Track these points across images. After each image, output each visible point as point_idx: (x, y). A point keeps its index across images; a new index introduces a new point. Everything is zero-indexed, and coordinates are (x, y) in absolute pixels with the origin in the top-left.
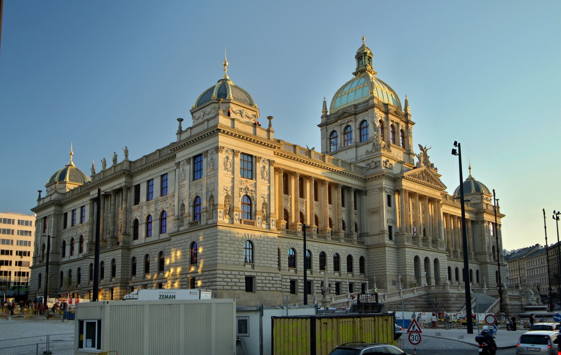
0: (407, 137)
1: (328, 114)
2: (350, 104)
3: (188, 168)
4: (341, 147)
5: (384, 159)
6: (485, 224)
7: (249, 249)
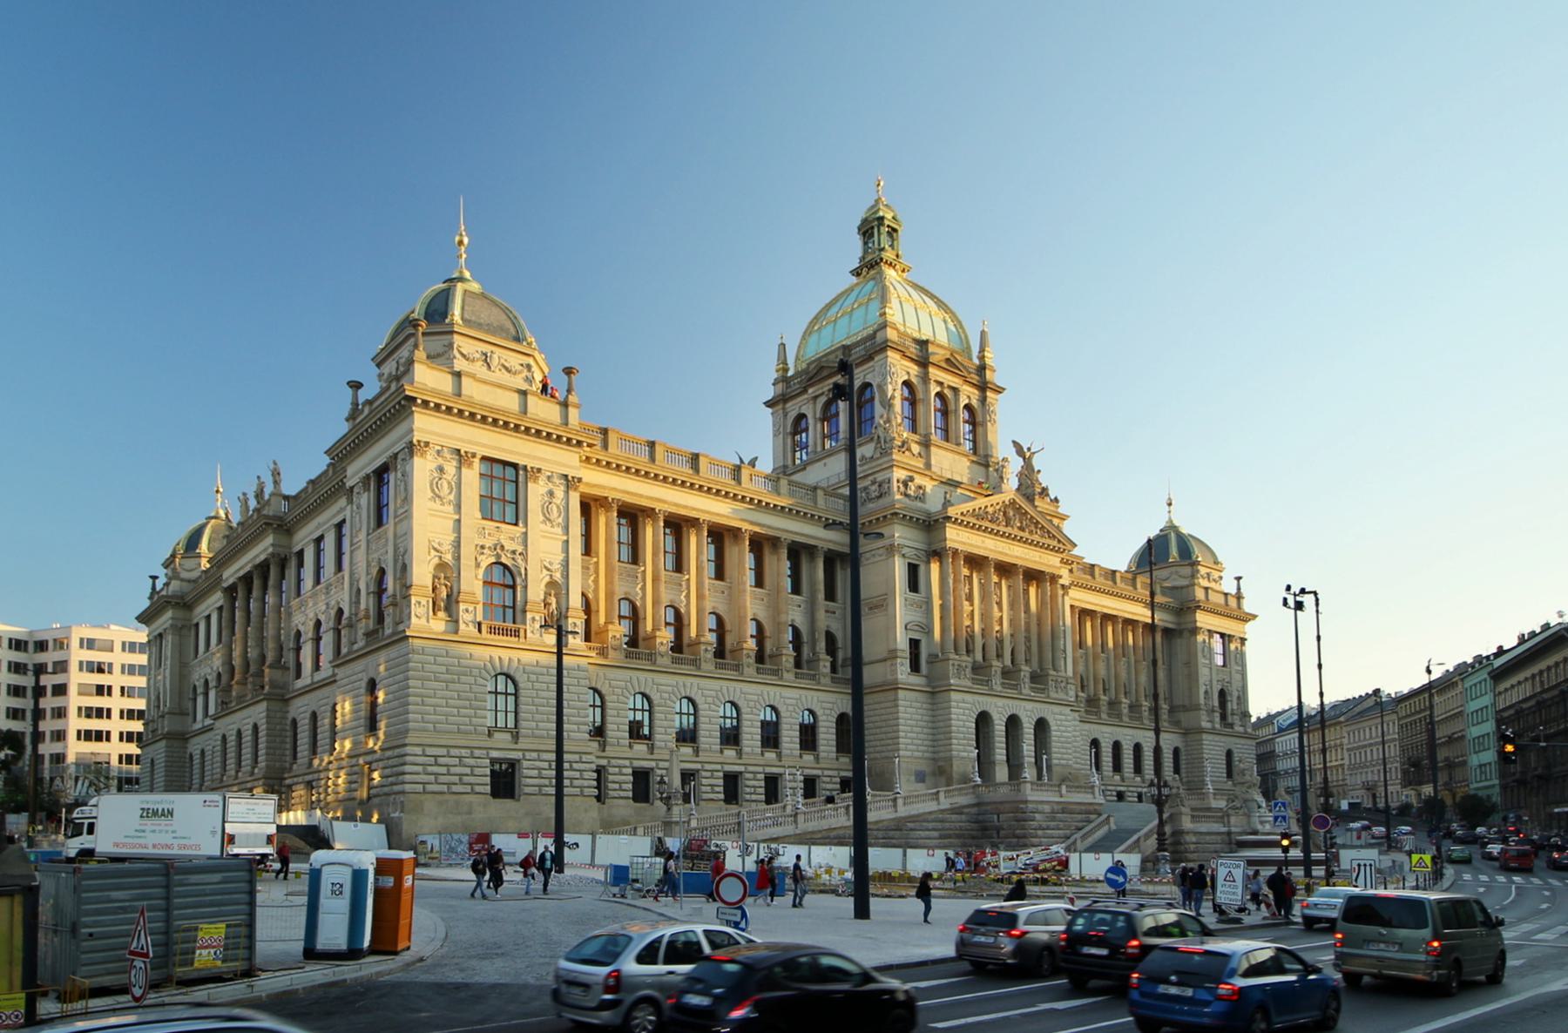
0: (984, 424)
1: (790, 373)
4: (815, 452)
5: (899, 474)
6: (1200, 638)
7: (506, 694)
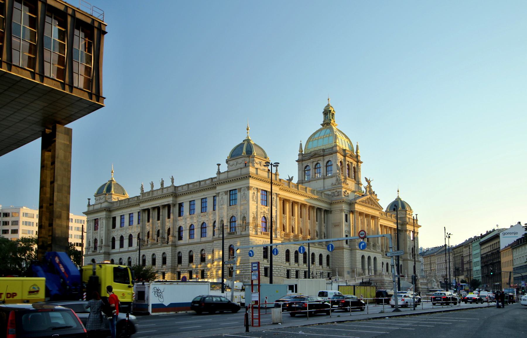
0: (358, 172)
1: (303, 153)
2: (319, 148)
3: (226, 198)
5: (344, 190)
6: (408, 232)
